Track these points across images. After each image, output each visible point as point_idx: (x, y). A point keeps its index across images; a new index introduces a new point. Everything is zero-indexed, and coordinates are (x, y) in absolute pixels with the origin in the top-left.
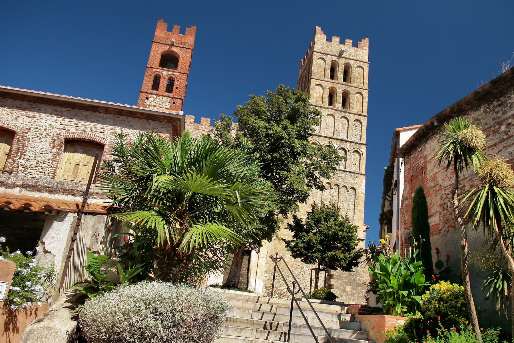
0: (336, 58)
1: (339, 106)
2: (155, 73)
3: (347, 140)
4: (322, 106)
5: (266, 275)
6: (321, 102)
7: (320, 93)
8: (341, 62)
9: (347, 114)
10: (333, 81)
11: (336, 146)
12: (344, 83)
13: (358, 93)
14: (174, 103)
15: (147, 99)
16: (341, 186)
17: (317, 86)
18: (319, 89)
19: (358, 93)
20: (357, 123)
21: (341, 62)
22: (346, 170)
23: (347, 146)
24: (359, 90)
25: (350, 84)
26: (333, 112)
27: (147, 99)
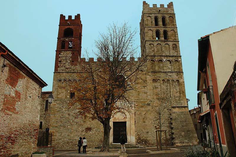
0: (157, 15)
1: (163, 39)
2: (62, 41)
3: (170, 55)
4: (153, 40)
5: (136, 133)
6: (152, 38)
7: (151, 34)
8: (160, 16)
9: (168, 42)
10: (157, 27)
11: (164, 60)
12: (163, 26)
13: (172, 30)
14: (74, 53)
15: (60, 54)
16: (171, 80)
17: (149, 31)
18: (150, 32)
19: (172, 30)
20: (174, 46)
21: (160, 16)
22: (172, 71)
23: (171, 59)
24: (172, 29)
25: (167, 26)
26: (160, 42)
27: (60, 54)
